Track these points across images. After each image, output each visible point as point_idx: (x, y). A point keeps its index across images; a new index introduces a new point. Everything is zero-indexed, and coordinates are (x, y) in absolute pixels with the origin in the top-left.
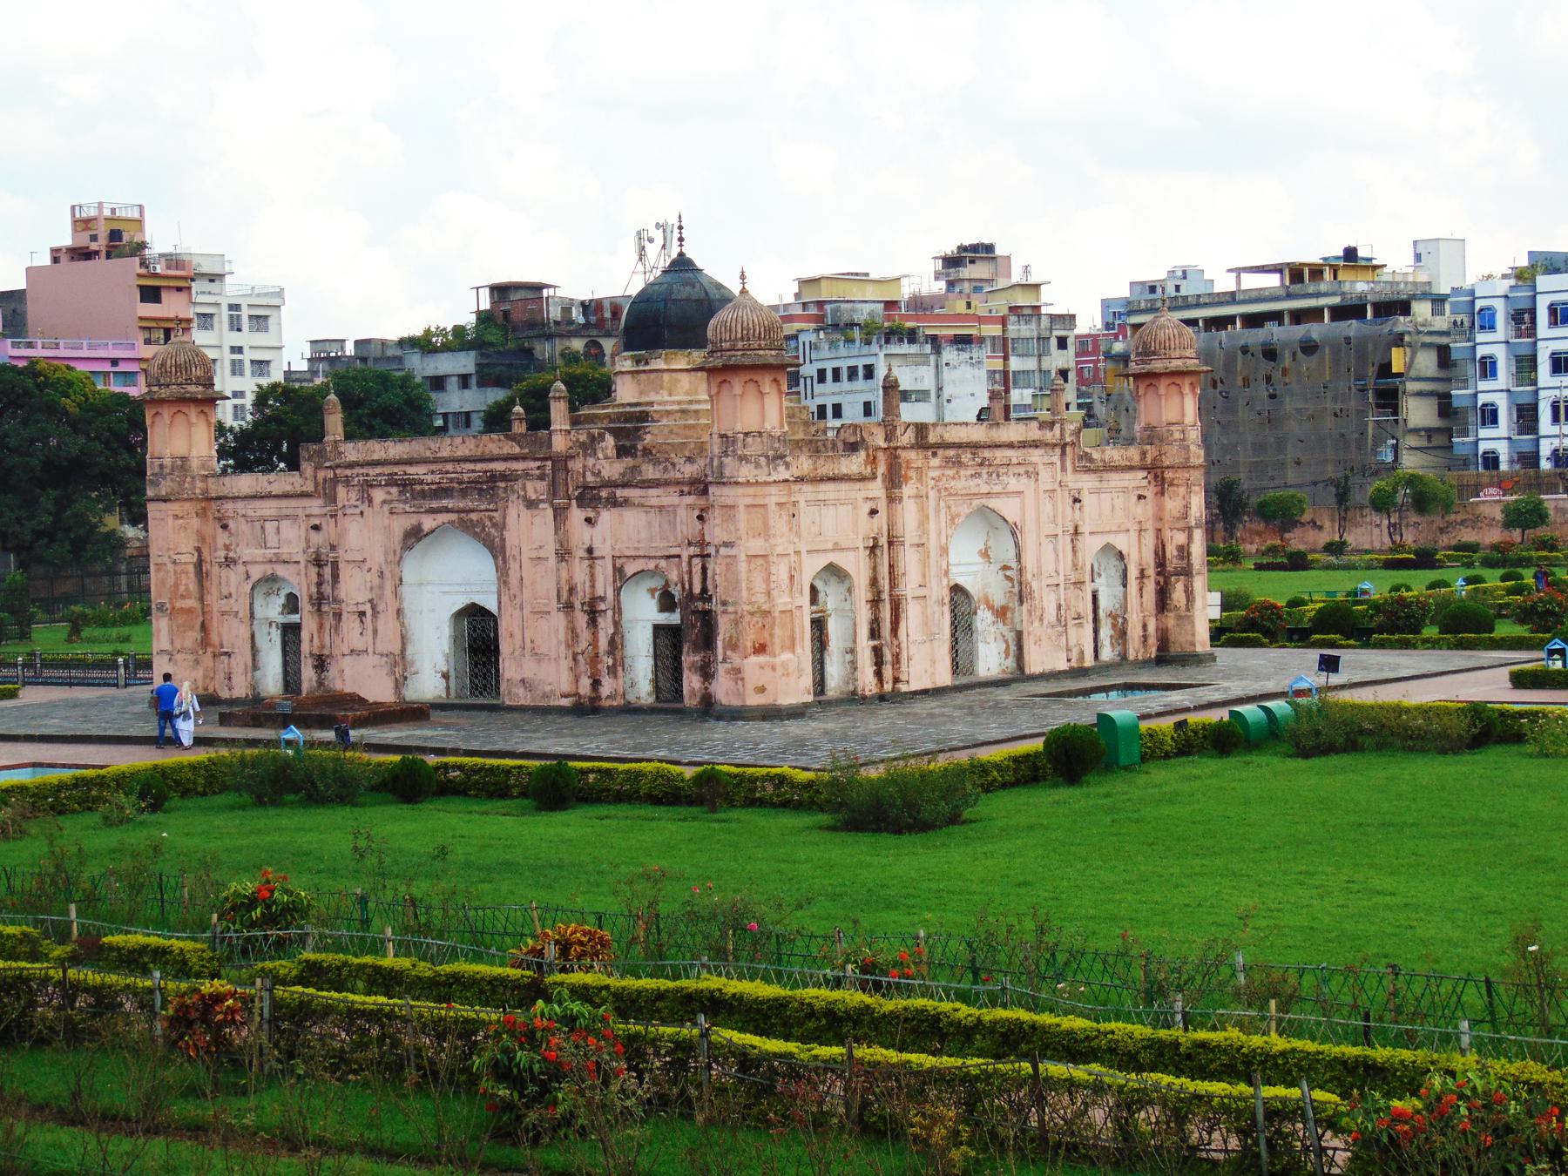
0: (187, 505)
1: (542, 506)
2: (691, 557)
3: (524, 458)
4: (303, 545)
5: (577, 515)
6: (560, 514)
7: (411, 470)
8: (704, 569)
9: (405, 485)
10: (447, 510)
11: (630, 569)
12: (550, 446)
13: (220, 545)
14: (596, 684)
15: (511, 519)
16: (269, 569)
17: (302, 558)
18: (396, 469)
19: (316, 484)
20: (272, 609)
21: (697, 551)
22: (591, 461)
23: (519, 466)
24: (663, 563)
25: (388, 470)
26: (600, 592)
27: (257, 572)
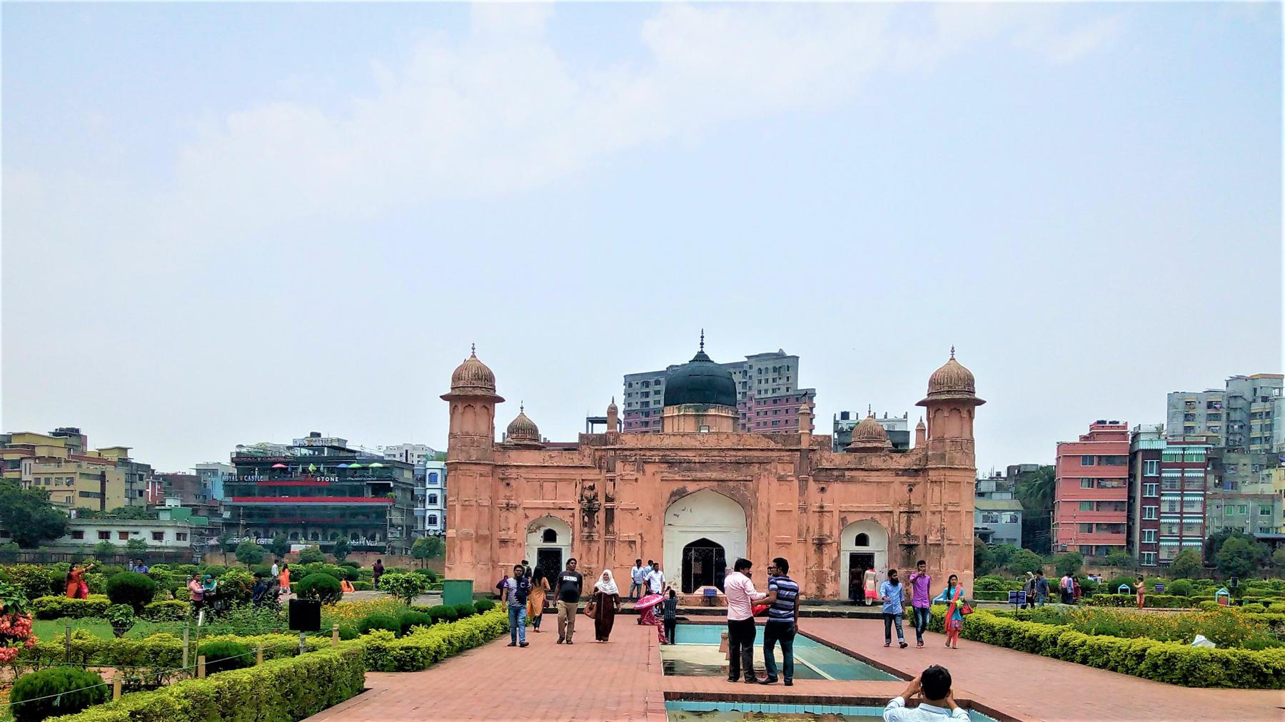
0: (488, 469)
5: (813, 486)
6: (803, 485)
8: (909, 521)
9: (671, 464)
11: (851, 519)
12: (799, 442)
13: (501, 494)
15: (763, 483)
16: (545, 514)
17: (577, 508)
20: (537, 541)
23: (775, 454)
24: (877, 517)
26: (826, 531)
27: (533, 515)
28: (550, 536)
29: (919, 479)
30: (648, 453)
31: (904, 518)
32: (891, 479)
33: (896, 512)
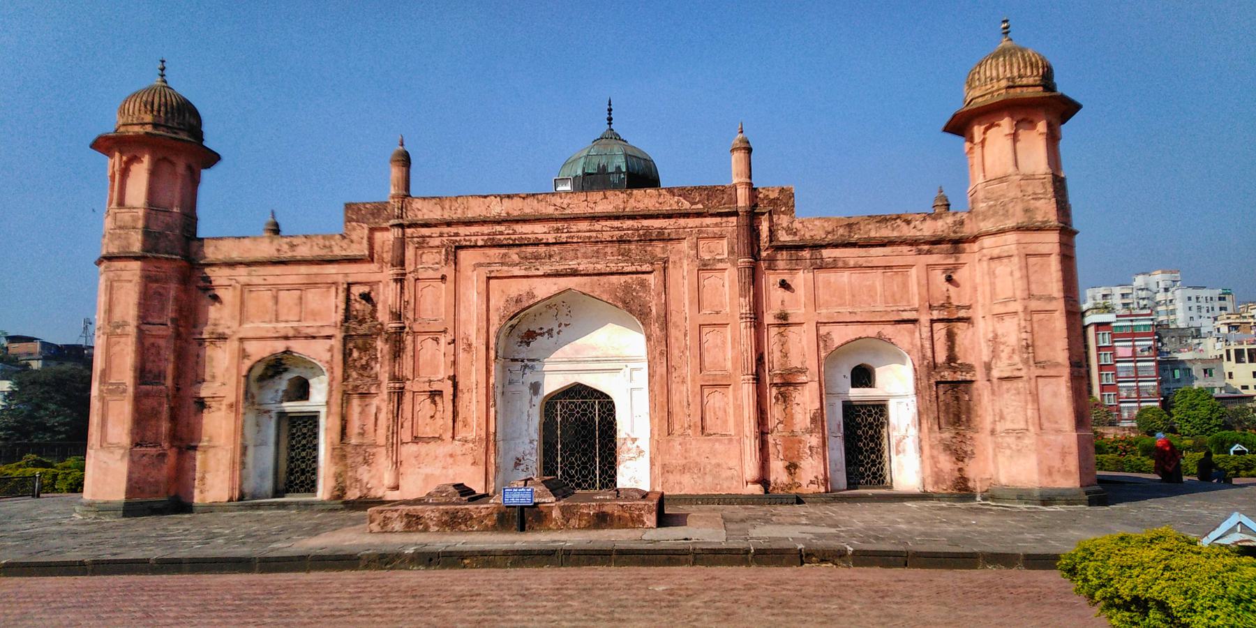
1: (720, 266)
2: (932, 321)
3: (699, 215)
4: (339, 317)
7: (520, 228)
8: (951, 337)
10: (574, 273)
14: (792, 468)
16: (280, 346)
18: (498, 228)
19: (371, 247)
21: (944, 314)
22: (784, 220)
23: (692, 222)
24: (888, 330)
25: (486, 229)
26: (795, 362)
27: (260, 351)
28: (301, 390)
29: (963, 258)
30: (463, 230)
31: (940, 330)
32: (910, 260)
33: (924, 319)
